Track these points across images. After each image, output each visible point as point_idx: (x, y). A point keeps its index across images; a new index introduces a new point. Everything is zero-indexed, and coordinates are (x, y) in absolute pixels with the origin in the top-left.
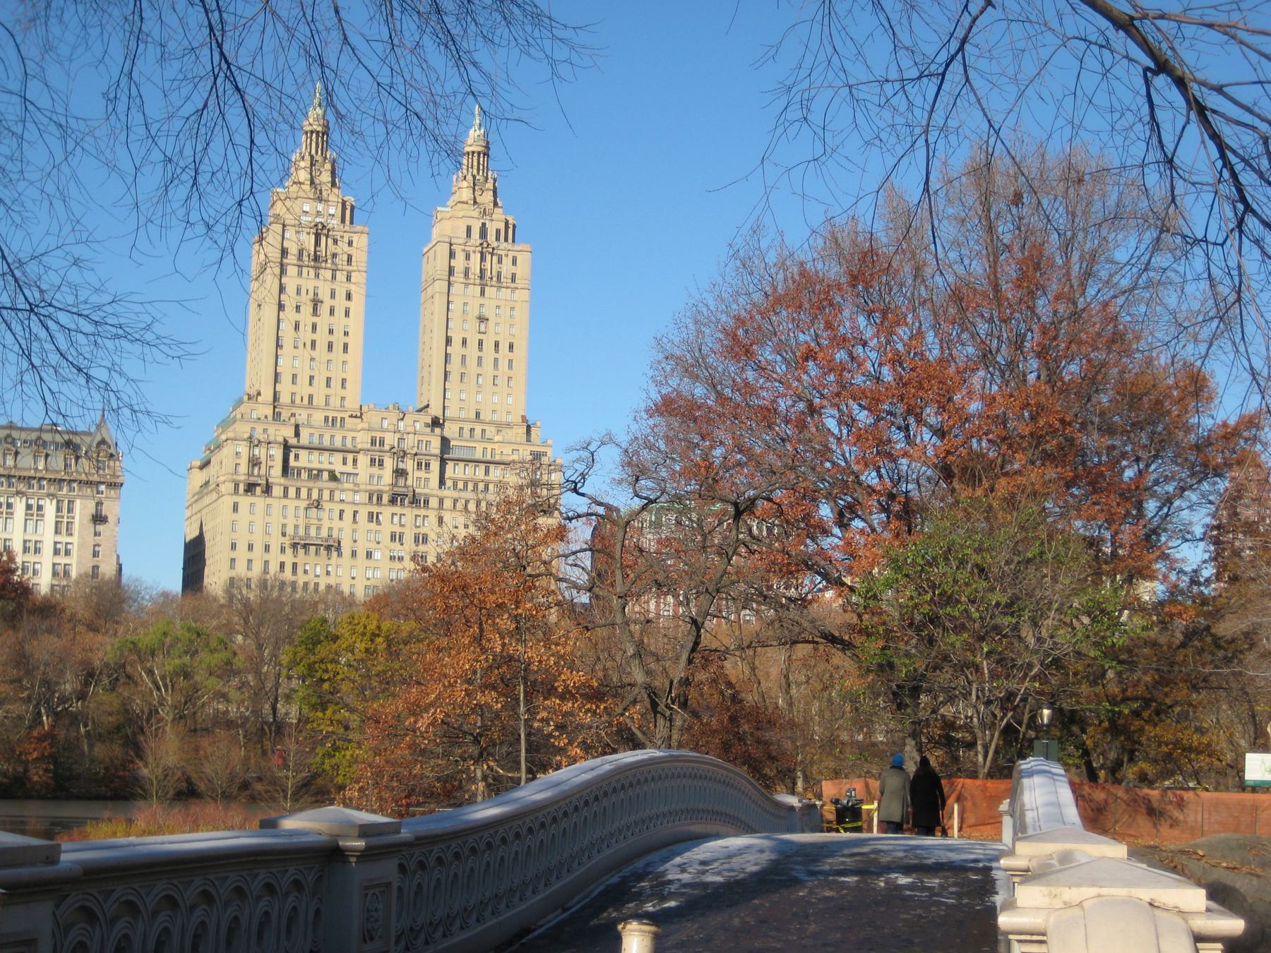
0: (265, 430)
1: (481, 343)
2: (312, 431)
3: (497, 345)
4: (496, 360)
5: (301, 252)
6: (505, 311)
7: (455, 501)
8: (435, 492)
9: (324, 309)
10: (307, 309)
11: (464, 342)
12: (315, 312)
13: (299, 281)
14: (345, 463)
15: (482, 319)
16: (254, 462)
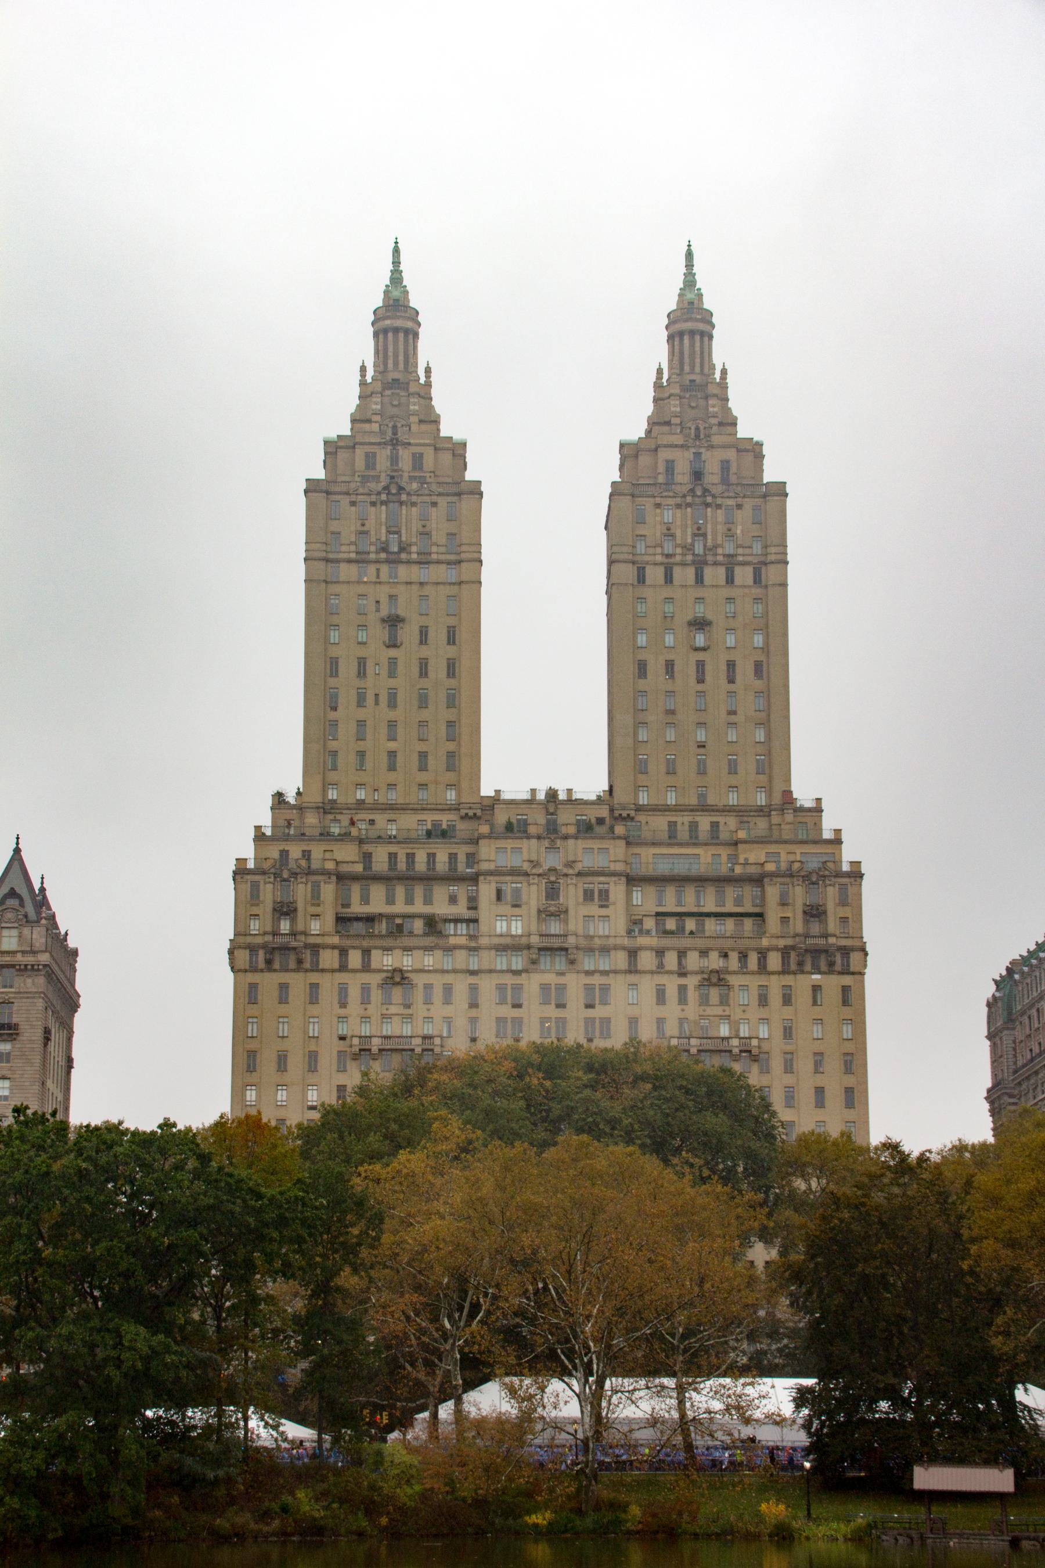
0: (307, 855)
1: (700, 665)
2: (393, 848)
3: (731, 665)
7: (660, 953)
8: (619, 941)
9: (408, 634)
10: (381, 633)
11: (670, 666)
12: (393, 644)
14: (453, 900)
16: (285, 910)
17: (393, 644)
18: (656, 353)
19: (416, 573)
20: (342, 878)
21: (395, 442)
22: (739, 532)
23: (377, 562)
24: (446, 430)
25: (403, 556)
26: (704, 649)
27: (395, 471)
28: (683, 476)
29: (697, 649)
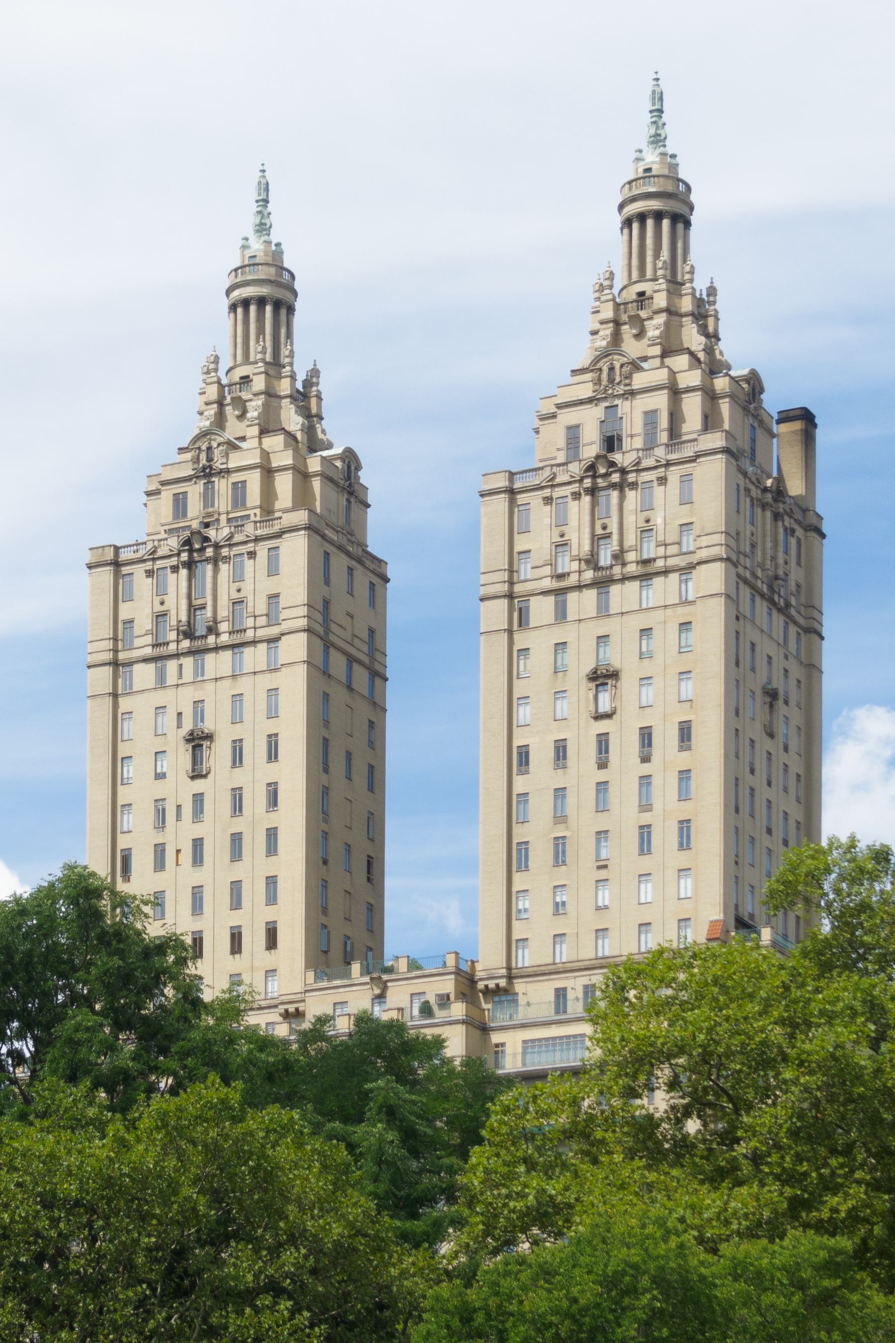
1: (603, 742)
4: (645, 780)
5: (160, 617)
6: (666, 639)
11: (561, 751)
13: (160, 697)
15: (603, 677)
21: (207, 473)
22: (659, 521)
23: (177, 656)
25: (211, 639)
26: (608, 716)
27: (209, 515)
29: (599, 717)
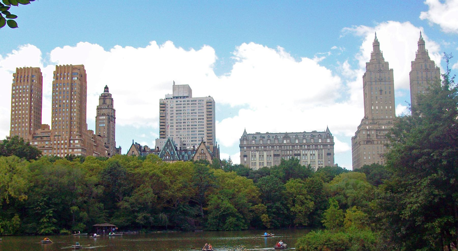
9: (383, 92)
17: (381, 94)
18: (416, 48)
19: (384, 83)
20: (377, 130)
21: (379, 63)
24: (385, 61)
28: (424, 68)
